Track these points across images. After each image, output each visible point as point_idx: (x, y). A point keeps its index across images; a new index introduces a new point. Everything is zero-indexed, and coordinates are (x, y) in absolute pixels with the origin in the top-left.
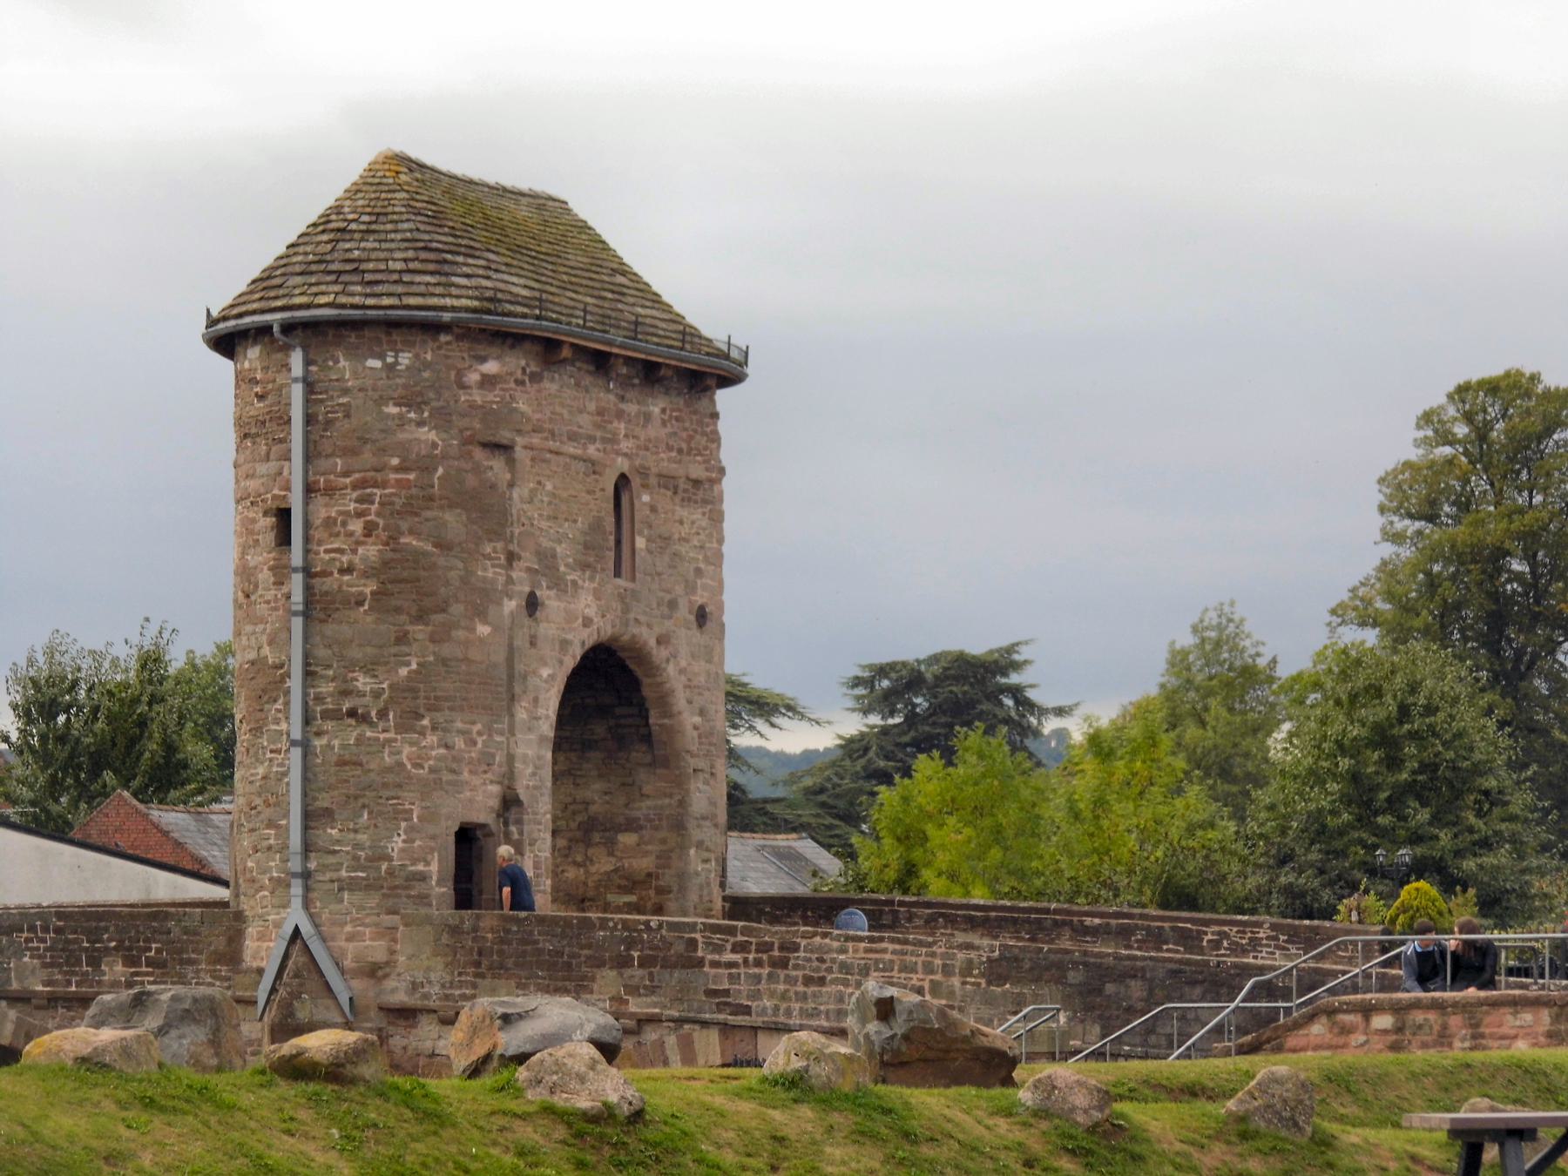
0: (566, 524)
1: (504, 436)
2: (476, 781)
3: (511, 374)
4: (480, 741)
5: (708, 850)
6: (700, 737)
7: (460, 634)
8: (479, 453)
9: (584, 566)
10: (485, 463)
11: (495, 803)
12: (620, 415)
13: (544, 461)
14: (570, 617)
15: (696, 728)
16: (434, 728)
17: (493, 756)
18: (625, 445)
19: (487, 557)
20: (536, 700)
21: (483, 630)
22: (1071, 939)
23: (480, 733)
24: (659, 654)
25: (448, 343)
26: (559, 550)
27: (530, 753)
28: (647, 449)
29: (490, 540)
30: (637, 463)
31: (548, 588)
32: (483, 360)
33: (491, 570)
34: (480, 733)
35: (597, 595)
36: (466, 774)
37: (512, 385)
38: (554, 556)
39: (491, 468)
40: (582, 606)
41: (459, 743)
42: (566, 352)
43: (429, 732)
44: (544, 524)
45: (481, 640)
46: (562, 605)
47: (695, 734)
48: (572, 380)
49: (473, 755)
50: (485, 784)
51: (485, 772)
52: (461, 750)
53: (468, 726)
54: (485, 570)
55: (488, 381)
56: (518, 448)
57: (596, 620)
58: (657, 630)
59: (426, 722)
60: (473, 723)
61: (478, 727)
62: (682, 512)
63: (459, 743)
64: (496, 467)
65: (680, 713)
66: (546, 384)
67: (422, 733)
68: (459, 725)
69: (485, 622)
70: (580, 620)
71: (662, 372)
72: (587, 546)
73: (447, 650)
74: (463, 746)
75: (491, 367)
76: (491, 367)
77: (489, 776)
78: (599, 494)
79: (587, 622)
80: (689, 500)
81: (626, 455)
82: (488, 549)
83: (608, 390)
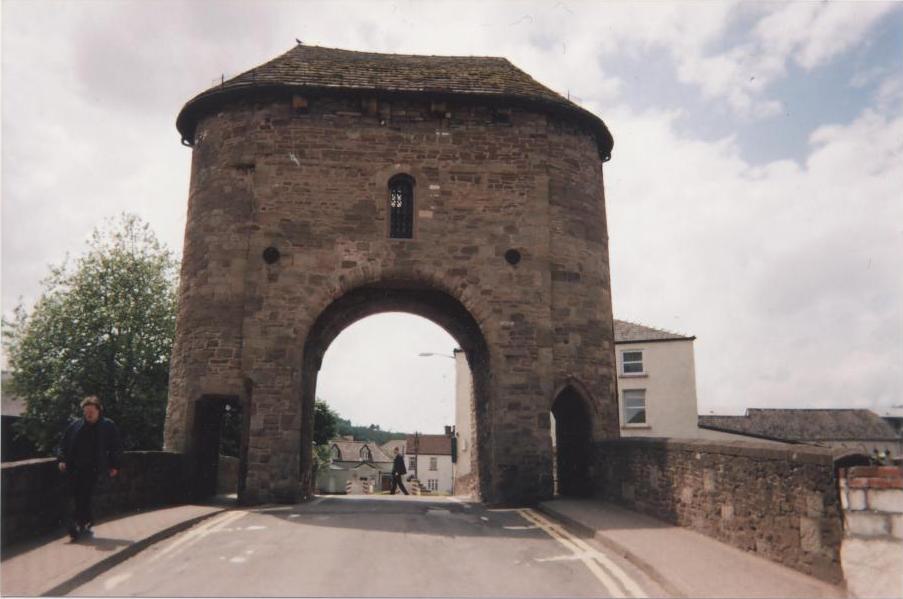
1: (247, 158)
6: (512, 333)
11: (240, 382)
16: (196, 338)
22: (693, 473)
24: (454, 283)
25: (222, 117)
28: (429, 157)
30: (421, 166)
37: (259, 129)
57: (359, 263)
58: (447, 266)
64: (248, 179)
72: (348, 218)
73: (204, 290)
79: (347, 264)
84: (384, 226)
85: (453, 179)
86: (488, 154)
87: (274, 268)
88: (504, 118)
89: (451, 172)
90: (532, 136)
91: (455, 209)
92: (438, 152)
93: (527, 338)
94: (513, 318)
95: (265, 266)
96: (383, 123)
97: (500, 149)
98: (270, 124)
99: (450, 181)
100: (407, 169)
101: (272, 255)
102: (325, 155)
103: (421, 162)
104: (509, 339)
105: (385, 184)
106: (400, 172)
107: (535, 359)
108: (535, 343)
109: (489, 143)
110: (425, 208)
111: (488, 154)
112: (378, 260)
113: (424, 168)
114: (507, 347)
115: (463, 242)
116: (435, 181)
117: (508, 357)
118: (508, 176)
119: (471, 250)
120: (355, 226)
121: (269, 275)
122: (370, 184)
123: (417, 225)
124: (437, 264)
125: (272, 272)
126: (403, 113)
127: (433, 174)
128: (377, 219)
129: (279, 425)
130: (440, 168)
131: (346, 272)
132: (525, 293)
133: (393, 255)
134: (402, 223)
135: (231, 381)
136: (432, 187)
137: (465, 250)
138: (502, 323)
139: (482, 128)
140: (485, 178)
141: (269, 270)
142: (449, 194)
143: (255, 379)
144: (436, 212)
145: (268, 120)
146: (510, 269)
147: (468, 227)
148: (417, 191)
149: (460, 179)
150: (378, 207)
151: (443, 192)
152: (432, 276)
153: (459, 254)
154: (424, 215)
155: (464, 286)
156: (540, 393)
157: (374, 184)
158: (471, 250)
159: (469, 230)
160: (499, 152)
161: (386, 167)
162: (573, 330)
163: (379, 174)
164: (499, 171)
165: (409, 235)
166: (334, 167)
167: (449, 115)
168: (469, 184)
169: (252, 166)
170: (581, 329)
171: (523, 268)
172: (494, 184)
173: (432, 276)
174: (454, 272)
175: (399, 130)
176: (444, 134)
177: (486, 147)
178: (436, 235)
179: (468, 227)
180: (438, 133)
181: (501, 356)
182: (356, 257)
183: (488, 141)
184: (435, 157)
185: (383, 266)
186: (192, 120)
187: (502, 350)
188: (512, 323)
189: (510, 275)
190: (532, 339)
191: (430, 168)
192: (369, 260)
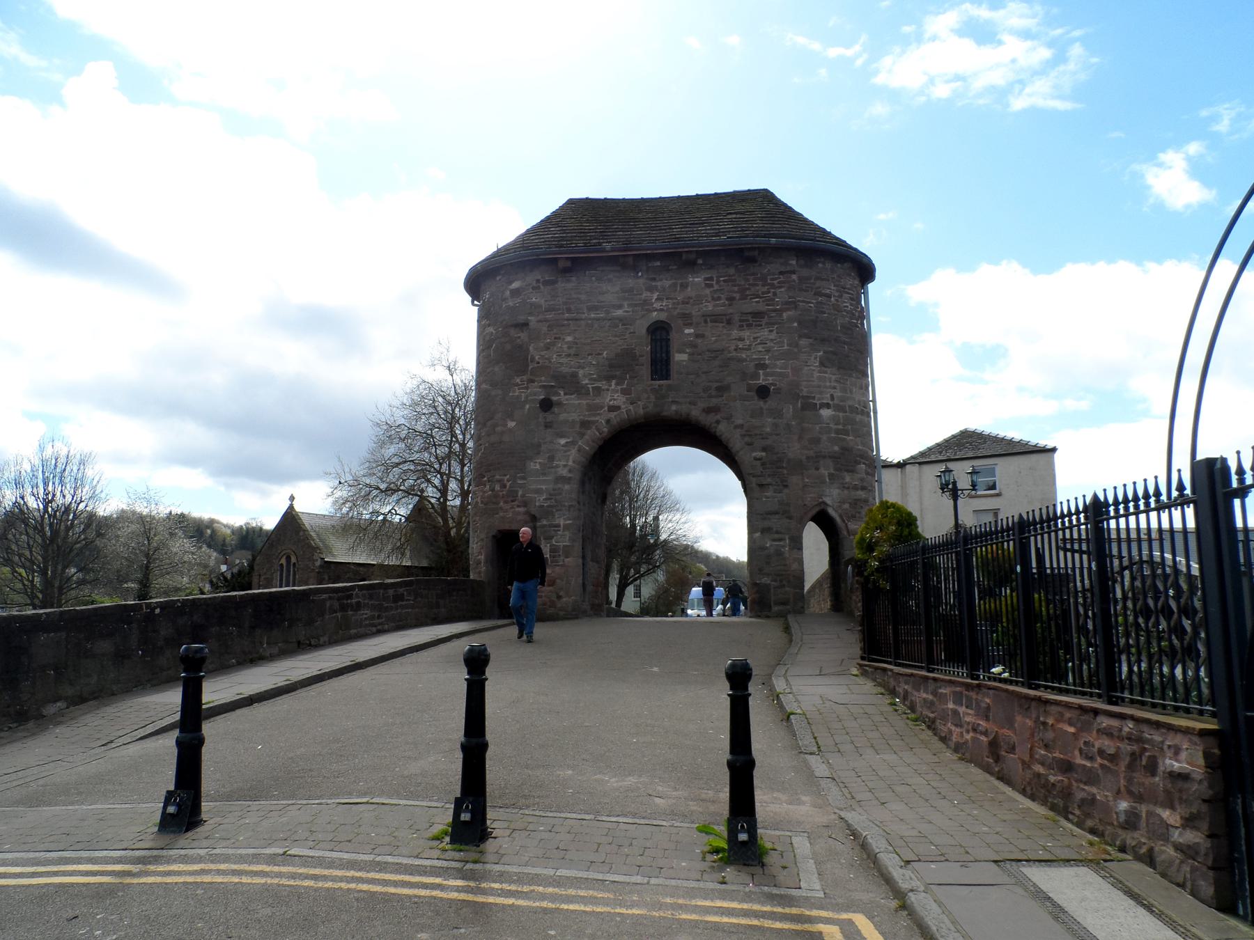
0: (590, 357)
2: (507, 507)
3: (530, 285)
4: (508, 484)
5: (777, 532)
6: (763, 464)
7: (499, 429)
8: (513, 332)
9: (608, 378)
10: (516, 336)
12: (651, 289)
13: (563, 325)
14: (594, 409)
15: (756, 459)
17: (517, 492)
18: (657, 305)
19: (517, 385)
20: (551, 458)
21: (511, 424)
23: (508, 481)
25: (500, 280)
26: (581, 372)
27: (544, 487)
29: (518, 376)
31: (565, 394)
32: (511, 283)
33: (518, 391)
34: (508, 481)
35: (624, 392)
36: (502, 504)
37: (531, 290)
38: (574, 375)
39: (519, 337)
40: (608, 400)
41: (497, 487)
42: (561, 264)
43: (487, 484)
44: (564, 360)
45: (510, 430)
46: (584, 402)
47: (758, 463)
48: (594, 278)
49: (504, 493)
50: (512, 508)
51: (512, 501)
52: (498, 491)
53: (502, 477)
54: (514, 392)
55: (516, 293)
56: (531, 324)
57: (623, 406)
58: (702, 405)
59: (485, 479)
60: (505, 475)
61: (508, 476)
62: (746, 334)
63: (497, 487)
65: (738, 452)
66: (561, 285)
67: (485, 486)
68: (498, 477)
69: (512, 421)
70: (606, 408)
71: (684, 257)
72: (611, 366)
74: (499, 489)
75: (515, 285)
76: (515, 285)
77: (516, 503)
78: (627, 336)
79: (613, 409)
80: (749, 326)
81: (662, 310)
82: (518, 380)
83: (638, 278)
84: (645, 371)
85: (706, 322)
86: (737, 296)
87: (550, 417)
88: (753, 260)
89: (703, 316)
90: (781, 273)
91: (708, 351)
92: (690, 298)
93: (778, 468)
94: (764, 449)
95: (541, 415)
96: (640, 274)
97: (749, 289)
98: (541, 285)
99: (703, 324)
100: (663, 316)
101: (546, 405)
102: (590, 309)
103: (677, 308)
104: (761, 469)
105: (644, 331)
106: (658, 319)
107: (786, 486)
108: (785, 472)
109: (740, 285)
110: (680, 351)
111: (737, 296)
112: (639, 403)
113: (678, 314)
114: (759, 476)
115: (717, 382)
116: (689, 325)
117: (761, 486)
118: (758, 315)
119: (723, 389)
120: (618, 373)
121: (545, 423)
122: (630, 333)
123: (674, 368)
124: (694, 404)
125: (548, 420)
126: (658, 264)
127: (687, 319)
128: (637, 365)
129: (561, 553)
130: (693, 312)
131: (612, 415)
132: (776, 425)
133: (653, 398)
134: (661, 366)
135: (520, 517)
136: (687, 331)
137: (719, 389)
138: (754, 454)
139: (732, 271)
140: (736, 318)
141: (545, 418)
142: (702, 336)
143: (537, 515)
144: (690, 354)
145: (538, 281)
146: (761, 403)
147: (720, 366)
148: (674, 336)
149: (711, 322)
150: (638, 354)
151: (697, 336)
152: (688, 415)
153: (714, 393)
154: (680, 357)
155: (718, 422)
156: (790, 518)
157: (634, 333)
158: (723, 389)
159: (721, 369)
160: (748, 293)
161: (643, 316)
162: (824, 457)
163: (638, 322)
164: (750, 310)
165: (666, 376)
166: (598, 319)
167: (700, 261)
168: (721, 325)
169: (525, 325)
170: (834, 457)
171: (771, 403)
172: (744, 323)
173: (688, 415)
174: (708, 411)
175: (654, 279)
176: (696, 279)
177: (736, 289)
178: (692, 376)
179: (720, 366)
180: (691, 279)
181: (754, 485)
182: (620, 400)
183: (737, 282)
184: (687, 303)
185: (643, 408)
186: (477, 282)
187: (754, 480)
188: (764, 454)
189: (761, 408)
190: (783, 467)
191: (686, 314)
192: (632, 404)
